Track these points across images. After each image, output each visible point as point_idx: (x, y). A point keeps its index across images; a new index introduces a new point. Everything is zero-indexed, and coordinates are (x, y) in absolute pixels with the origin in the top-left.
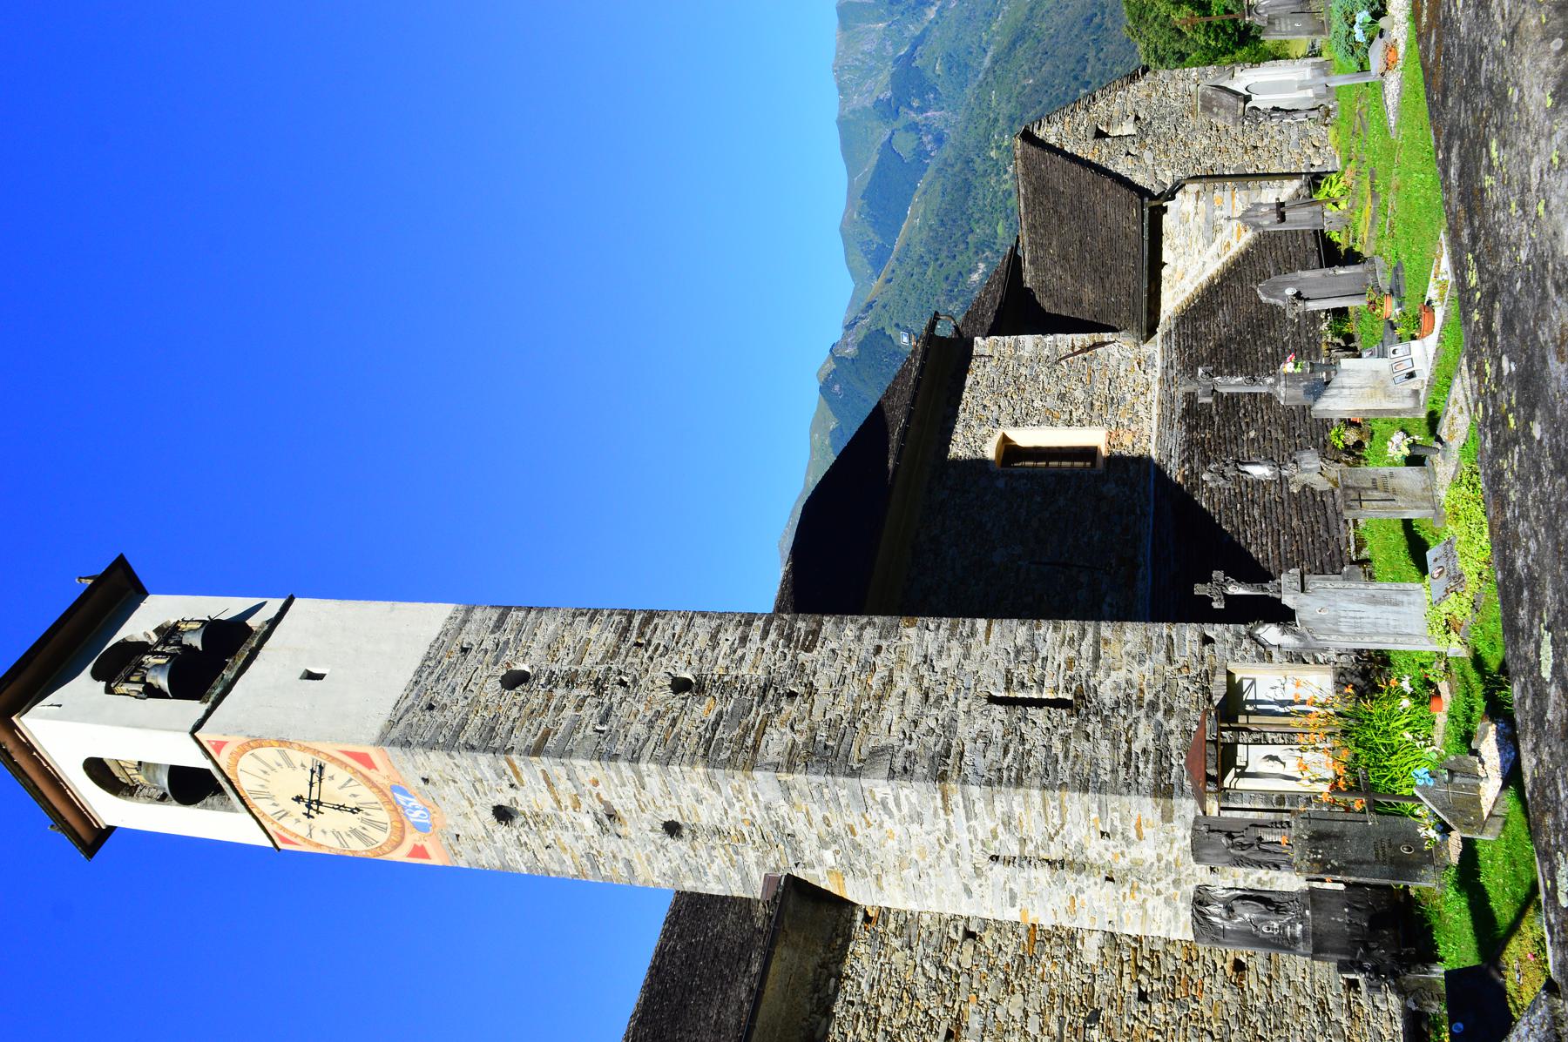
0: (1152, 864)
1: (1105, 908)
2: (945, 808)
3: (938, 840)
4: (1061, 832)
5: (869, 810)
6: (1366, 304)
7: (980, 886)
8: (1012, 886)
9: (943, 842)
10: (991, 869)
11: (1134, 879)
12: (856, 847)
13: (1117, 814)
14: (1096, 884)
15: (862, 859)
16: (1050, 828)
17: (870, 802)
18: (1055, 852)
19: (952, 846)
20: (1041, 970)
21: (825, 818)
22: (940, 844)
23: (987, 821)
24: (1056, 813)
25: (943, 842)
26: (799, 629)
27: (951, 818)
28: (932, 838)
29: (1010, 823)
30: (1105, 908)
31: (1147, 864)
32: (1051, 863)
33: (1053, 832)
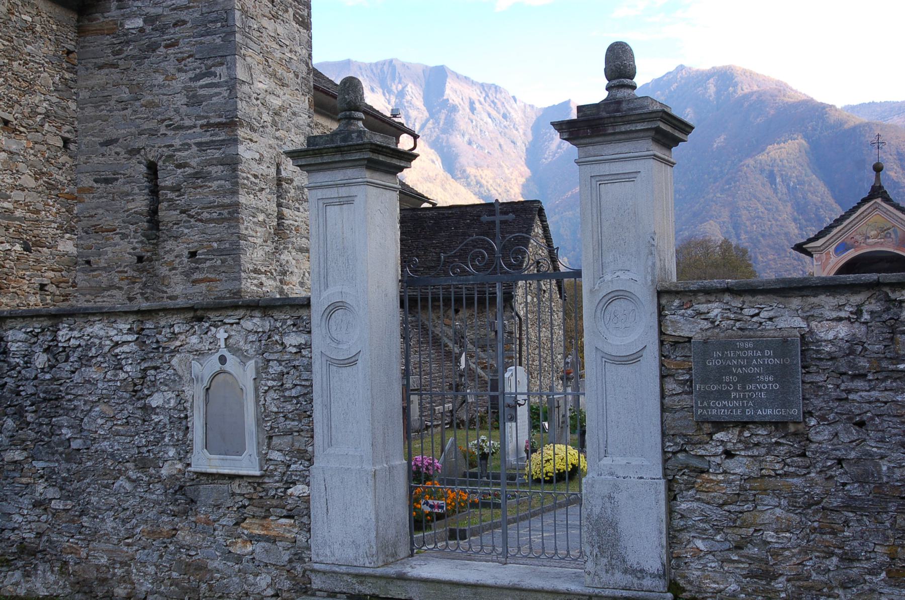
0: (166, 292)
1: (106, 257)
2: (209, 125)
3: (170, 119)
4: (192, 220)
5: (199, 62)
6: (883, 347)
7: (117, 154)
8: (121, 181)
9: (166, 123)
10: (140, 163)
11: (144, 279)
12: (153, 47)
13: (219, 262)
14: (134, 249)
15: (136, 52)
16: (196, 210)
17: (209, 62)
18: (166, 215)
19: (163, 130)
20: (51, 203)
21: (184, 22)
22: (165, 120)
23: (197, 159)
24: (215, 215)
25: (166, 123)
26: (304, 10)
27: (198, 130)
28: (172, 113)
29: (198, 179)
30: (106, 257)
31: (165, 289)
32: (153, 212)
33: (193, 212)
